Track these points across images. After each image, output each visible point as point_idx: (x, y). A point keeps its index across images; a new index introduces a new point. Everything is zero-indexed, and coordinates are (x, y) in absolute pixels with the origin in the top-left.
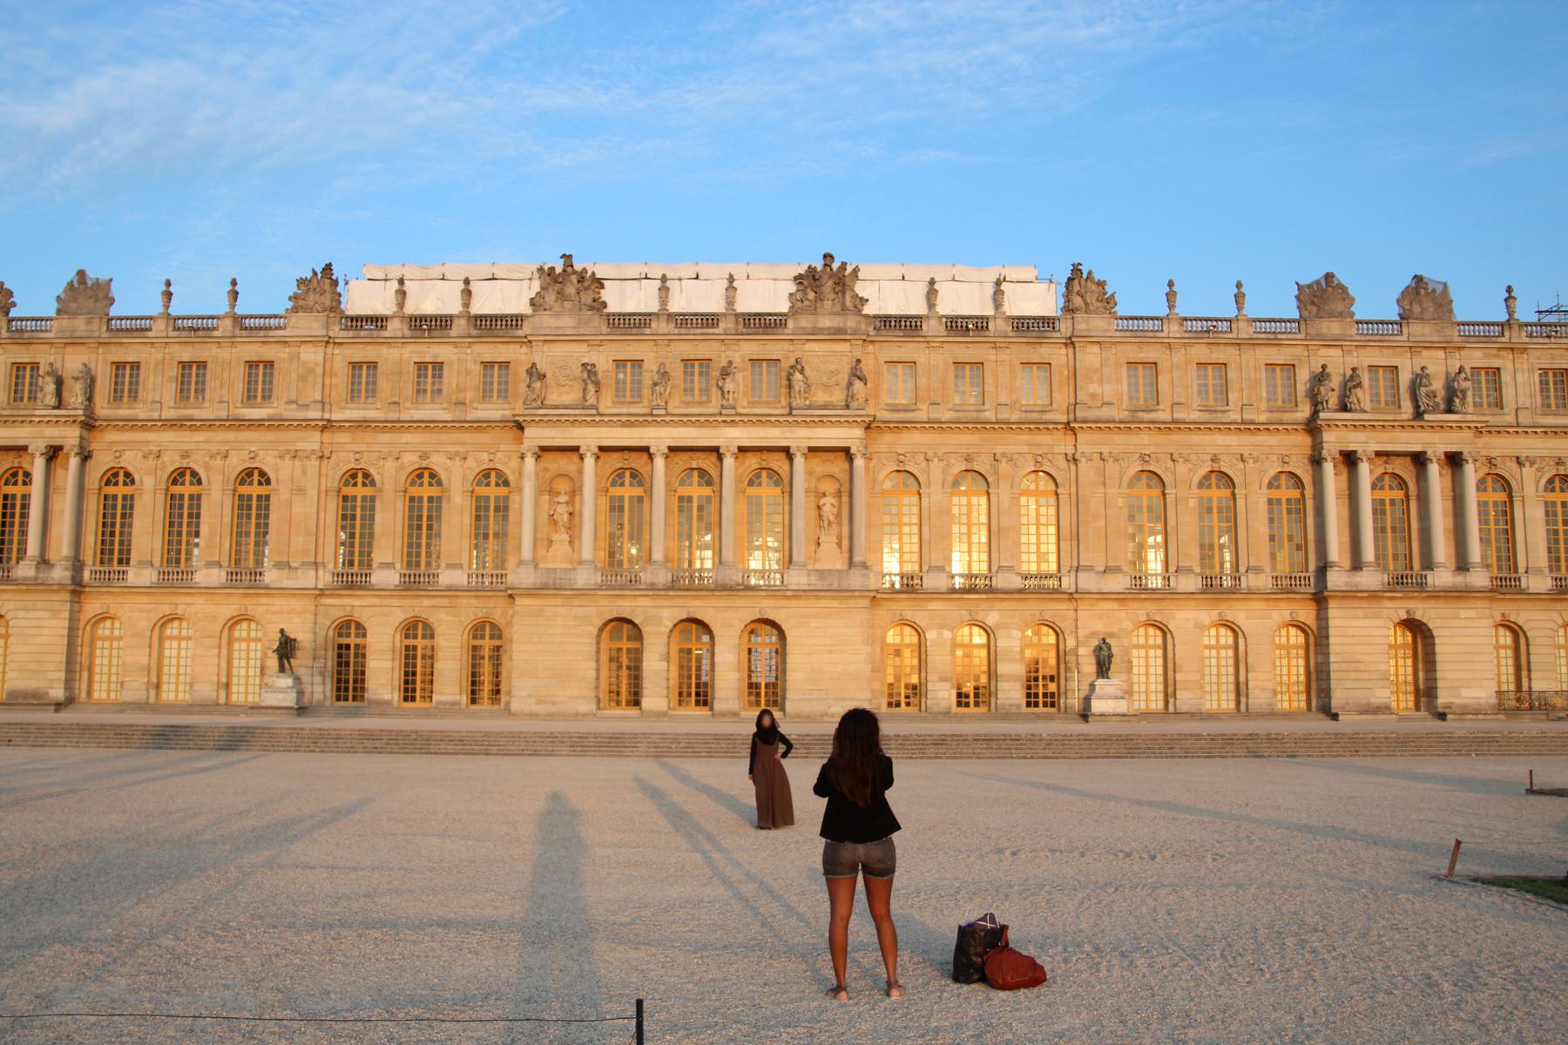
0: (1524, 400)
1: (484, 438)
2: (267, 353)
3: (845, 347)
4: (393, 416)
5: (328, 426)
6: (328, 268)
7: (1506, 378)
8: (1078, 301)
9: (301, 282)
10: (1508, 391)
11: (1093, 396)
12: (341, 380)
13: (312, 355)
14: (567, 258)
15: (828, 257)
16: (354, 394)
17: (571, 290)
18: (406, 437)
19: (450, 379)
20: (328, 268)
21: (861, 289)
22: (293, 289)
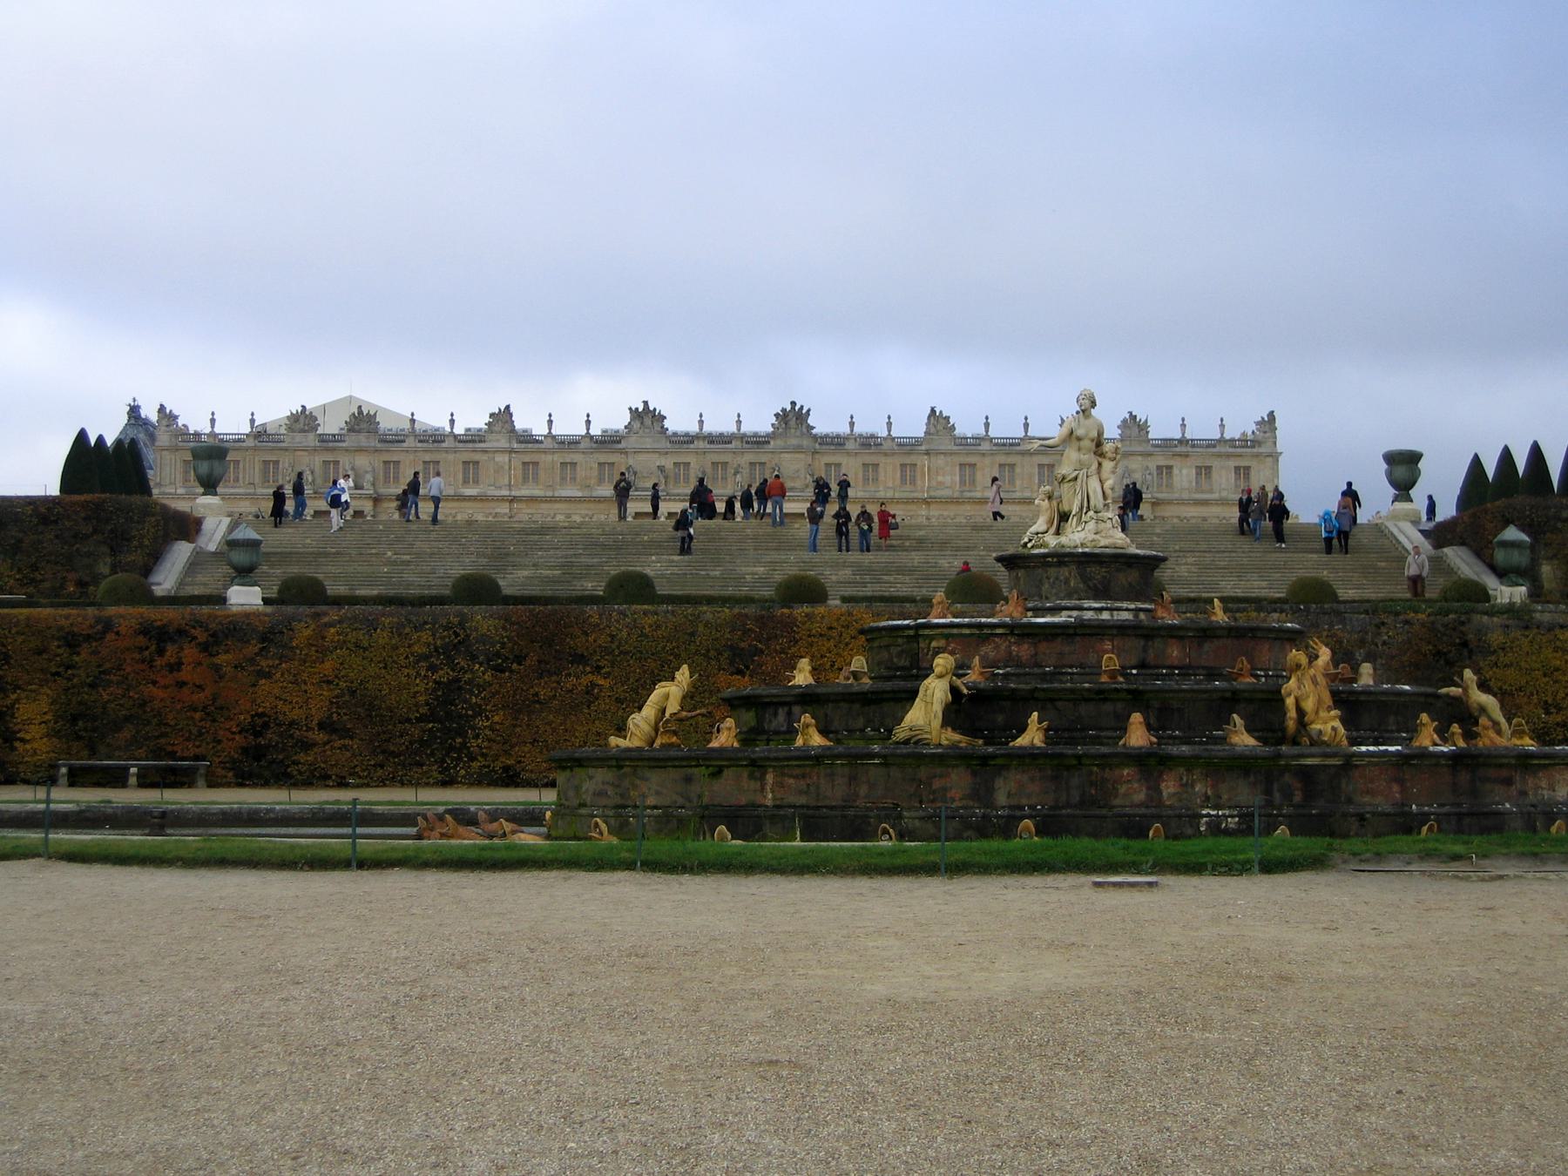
0: (1185, 484)
1: (602, 506)
2: (477, 457)
3: (802, 456)
4: (550, 494)
5: (513, 500)
6: (508, 407)
7: (1175, 471)
8: (933, 430)
9: (492, 415)
10: (1176, 479)
11: (940, 483)
12: (517, 470)
13: (502, 459)
14: (646, 403)
15: (793, 403)
16: (525, 479)
17: (648, 421)
18: (557, 506)
19: (581, 473)
20: (508, 407)
21: (811, 421)
22: (487, 419)
